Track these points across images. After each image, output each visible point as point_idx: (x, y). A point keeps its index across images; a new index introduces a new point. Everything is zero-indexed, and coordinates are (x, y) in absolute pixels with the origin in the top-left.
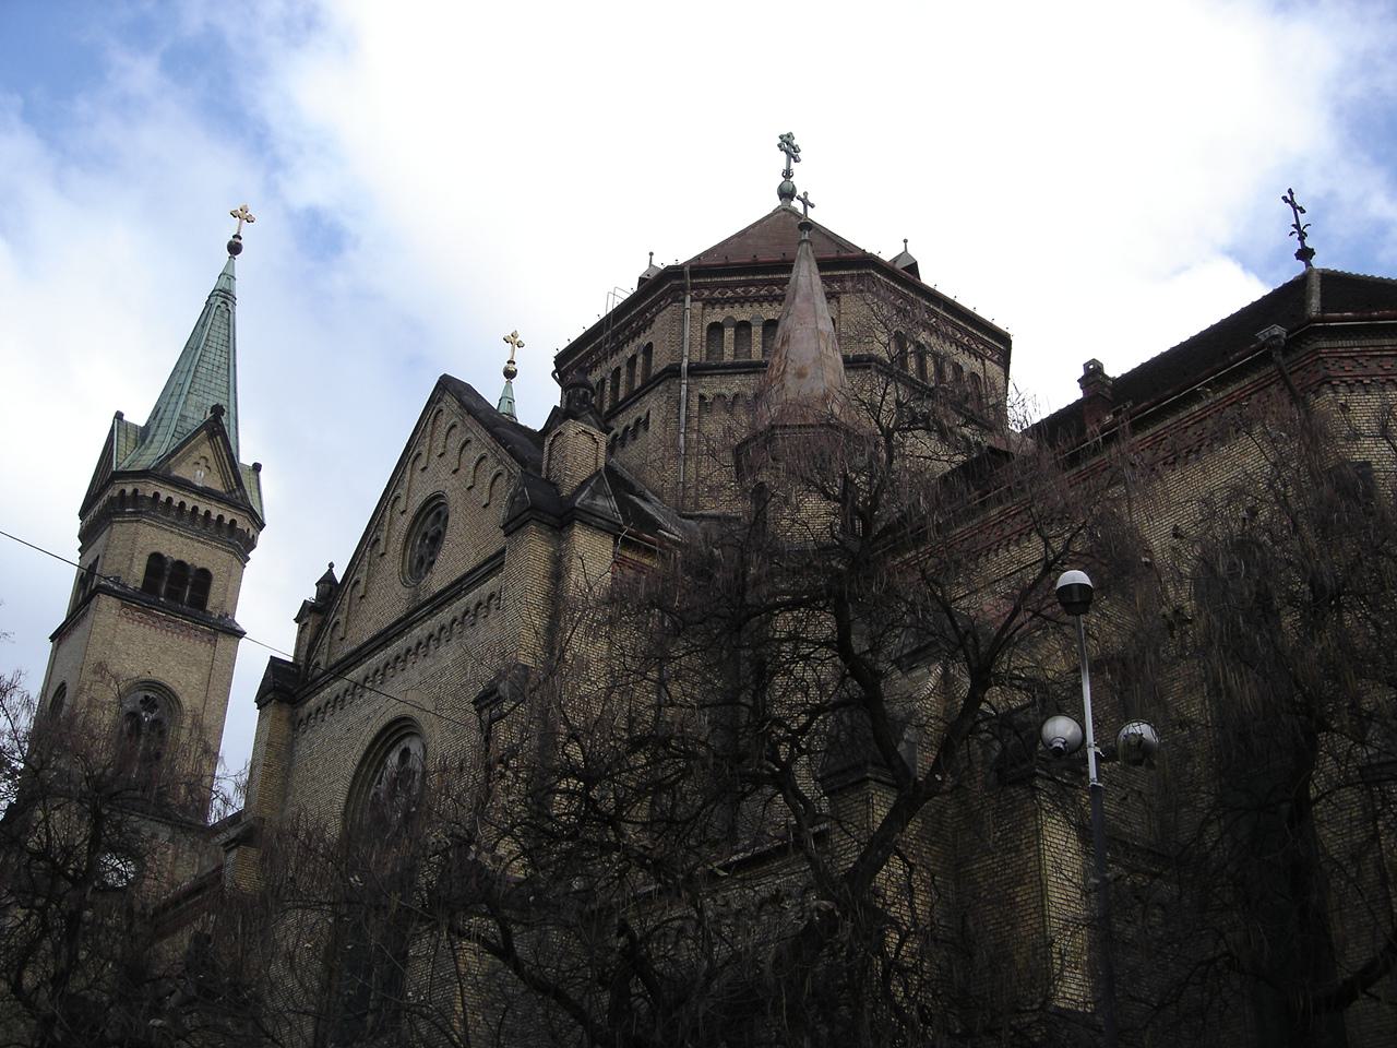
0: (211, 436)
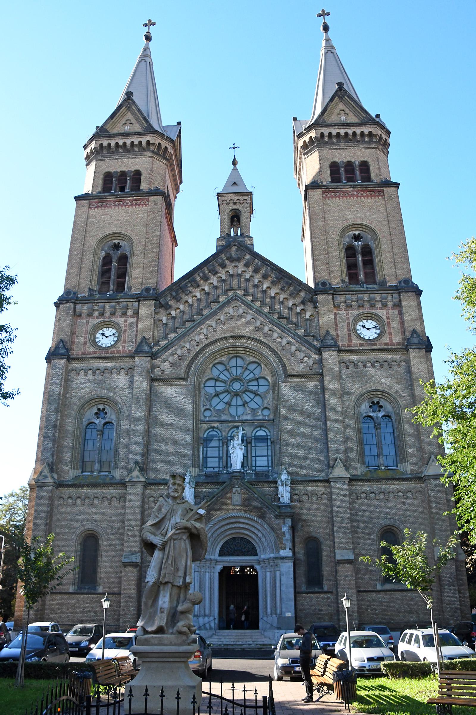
0: (341, 98)
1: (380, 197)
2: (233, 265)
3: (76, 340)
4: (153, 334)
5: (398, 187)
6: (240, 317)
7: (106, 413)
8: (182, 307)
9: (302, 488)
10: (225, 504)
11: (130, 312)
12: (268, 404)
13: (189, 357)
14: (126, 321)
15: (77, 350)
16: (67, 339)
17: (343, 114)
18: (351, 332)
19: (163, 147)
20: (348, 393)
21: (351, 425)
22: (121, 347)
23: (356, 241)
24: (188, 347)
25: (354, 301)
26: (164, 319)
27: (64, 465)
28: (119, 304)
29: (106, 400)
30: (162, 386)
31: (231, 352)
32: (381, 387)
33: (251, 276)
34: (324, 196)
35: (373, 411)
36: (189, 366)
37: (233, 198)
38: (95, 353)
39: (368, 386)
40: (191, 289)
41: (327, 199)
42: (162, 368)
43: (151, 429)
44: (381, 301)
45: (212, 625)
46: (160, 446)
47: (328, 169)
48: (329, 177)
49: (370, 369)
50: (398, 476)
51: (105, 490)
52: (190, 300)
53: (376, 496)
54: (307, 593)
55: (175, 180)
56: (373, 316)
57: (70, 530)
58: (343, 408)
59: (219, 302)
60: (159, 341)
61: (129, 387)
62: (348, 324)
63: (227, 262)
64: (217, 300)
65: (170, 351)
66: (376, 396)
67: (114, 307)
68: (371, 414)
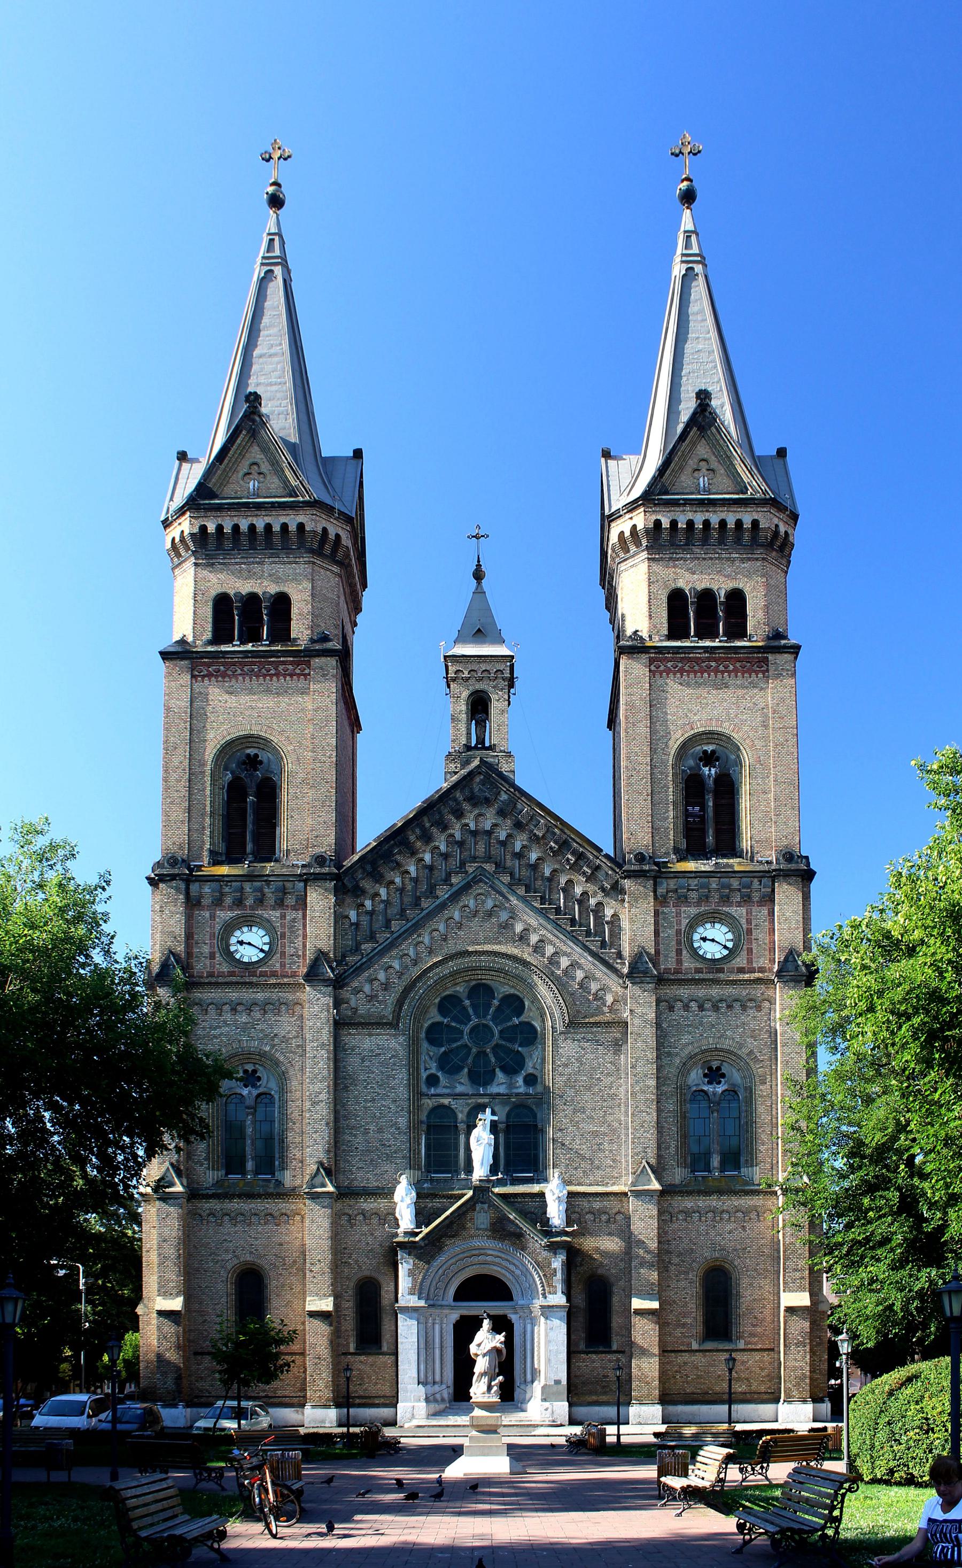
1: (760, 675)
2: (477, 812)
3: (196, 950)
4: (335, 943)
5: (797, 654)
6: (490, 914)
7: (259, 1079)
8: (383, 892)
9: (585, 1204)
10: (464, 1228)
11: (290, 900)
12: (534, 1068)
13: (399, 986)
14: (283, 917)
15: (201, 967)
16: (180, 949)
17: (704, 470)
18: (683, 947)
19: (332, 536)
20: (669, 1054)
21: (671, 1106)
22: (278, 965)
23: (705, 766)
24: (397, 967)
25: (693, 890)
26: (353, 915)
27: (196, 1163)
28: (268, 885)
29: (257, 1057)
30: (354, 1035)
31: (472, 977)
32: (726, 1044)
33: (509, 836)
34: (653, 668)
35: (710, 1083)
36: (400, 1003)
37: (475, 667)
38: (232, 974)
39: (704, 1042)
40: (398, 857)
41: (657, 675)
42: (353, 1003)
43: (338, 1107)
44: (739, 890)
45: (446, 1396)
46: (355, 1135)
47: (665, 605)
48: (666, 625)
49: (709, 1013)
50: (738, 1188)
51: (268, 1203)
52: (398, 880)
53: (700, 1217)
54: (587, 1353)
55: (352, 586)
56: (723, 917)
57: (217, 1262)
58: (658, 1078)
59: (451, 885)
60: (344, 956)
61: (298, 1037)
62: (678, 932)
63: (466, 806)
64: (447, 881)
65: (366, 974)
66: (717, 1058)
67: (261, 890)
68: (705, 1088)
